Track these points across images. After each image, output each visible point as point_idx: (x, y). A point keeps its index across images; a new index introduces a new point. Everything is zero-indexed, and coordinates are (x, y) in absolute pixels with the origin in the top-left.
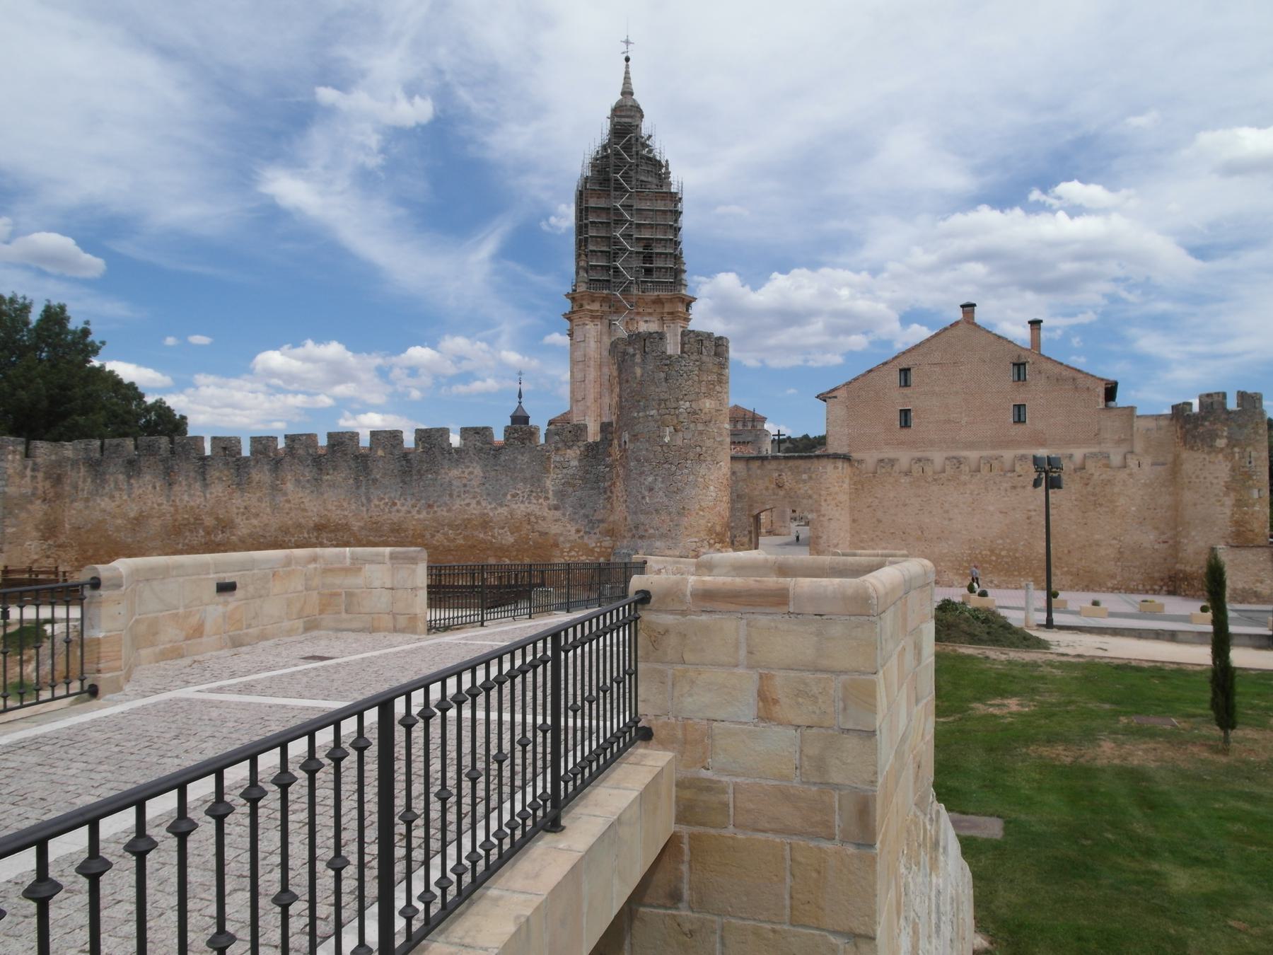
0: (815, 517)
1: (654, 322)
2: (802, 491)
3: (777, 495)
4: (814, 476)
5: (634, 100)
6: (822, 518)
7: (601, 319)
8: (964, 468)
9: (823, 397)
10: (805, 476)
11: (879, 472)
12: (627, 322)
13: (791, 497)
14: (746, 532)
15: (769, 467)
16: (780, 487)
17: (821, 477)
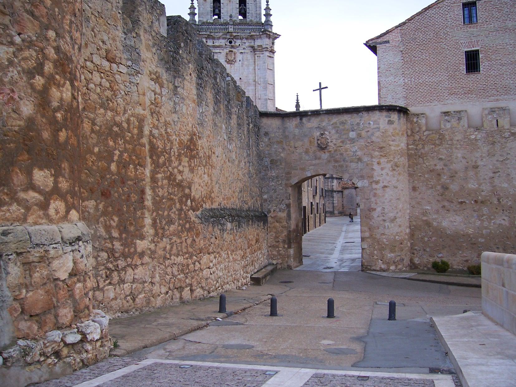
1: (247, 53)
3: (319, 159)
4: (364, 133)
6: (374, 186)
10: (352, 135)
12: (227, 54)
13: (336, 161)
14: (283, 206)
16: (322, 148)
17: (373, 134)
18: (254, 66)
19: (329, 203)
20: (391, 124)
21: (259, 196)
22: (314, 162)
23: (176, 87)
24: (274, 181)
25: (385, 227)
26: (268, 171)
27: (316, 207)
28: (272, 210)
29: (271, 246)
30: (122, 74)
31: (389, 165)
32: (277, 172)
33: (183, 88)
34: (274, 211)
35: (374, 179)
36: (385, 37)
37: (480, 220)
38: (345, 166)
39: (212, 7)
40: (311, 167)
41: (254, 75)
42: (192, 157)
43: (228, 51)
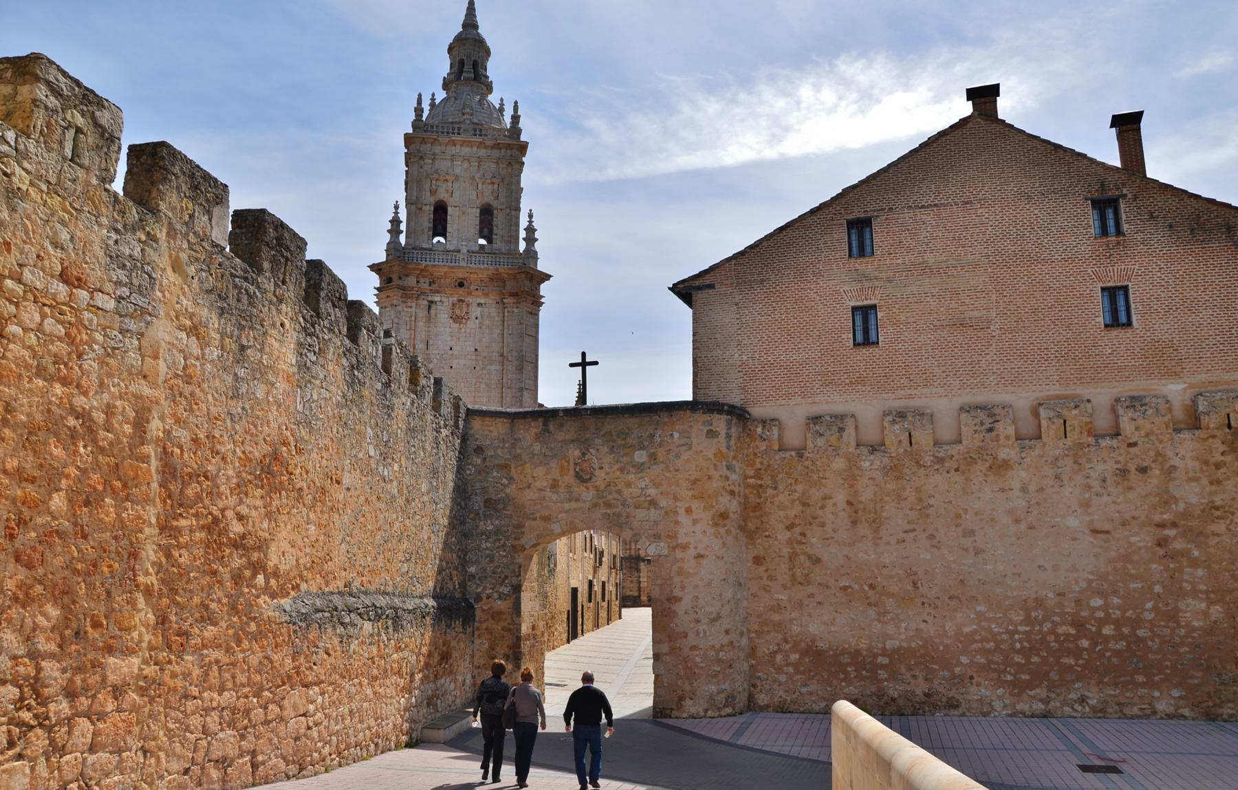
0: (665, 552)
2: (637, 492)
3: (577, 500)
5: (478, 34)
7: (417, 299)
8: (1006, 429)
9: (685, 290)
10: (640, 456)
11: (810, 445)
12: (453, 305)
13: (608, 505)
15: (561, 436)
17: (678, 456)
18: (501, 327)
19: (632, 582)
20: (713, 437)
21: (456, 569)
22: (567, 506)
23: (243, 348)
24: (491, 540)
25: (698, 633)
26: (480, 520)
27: (600, 590)
28: (484, 596)
29: (479, 667)
30: (100, 312)
31: (709, 515)
32: (497, 522)
33: (261, 350)
34: (488, 598)
35: (680, 541)
36: (707, 277)
37: (879, 621)
38: (624, 514)
39: (431, 221)
40: (560, 516)
41: (501, 344)
42: (276, 489)
43: (455, 299)
